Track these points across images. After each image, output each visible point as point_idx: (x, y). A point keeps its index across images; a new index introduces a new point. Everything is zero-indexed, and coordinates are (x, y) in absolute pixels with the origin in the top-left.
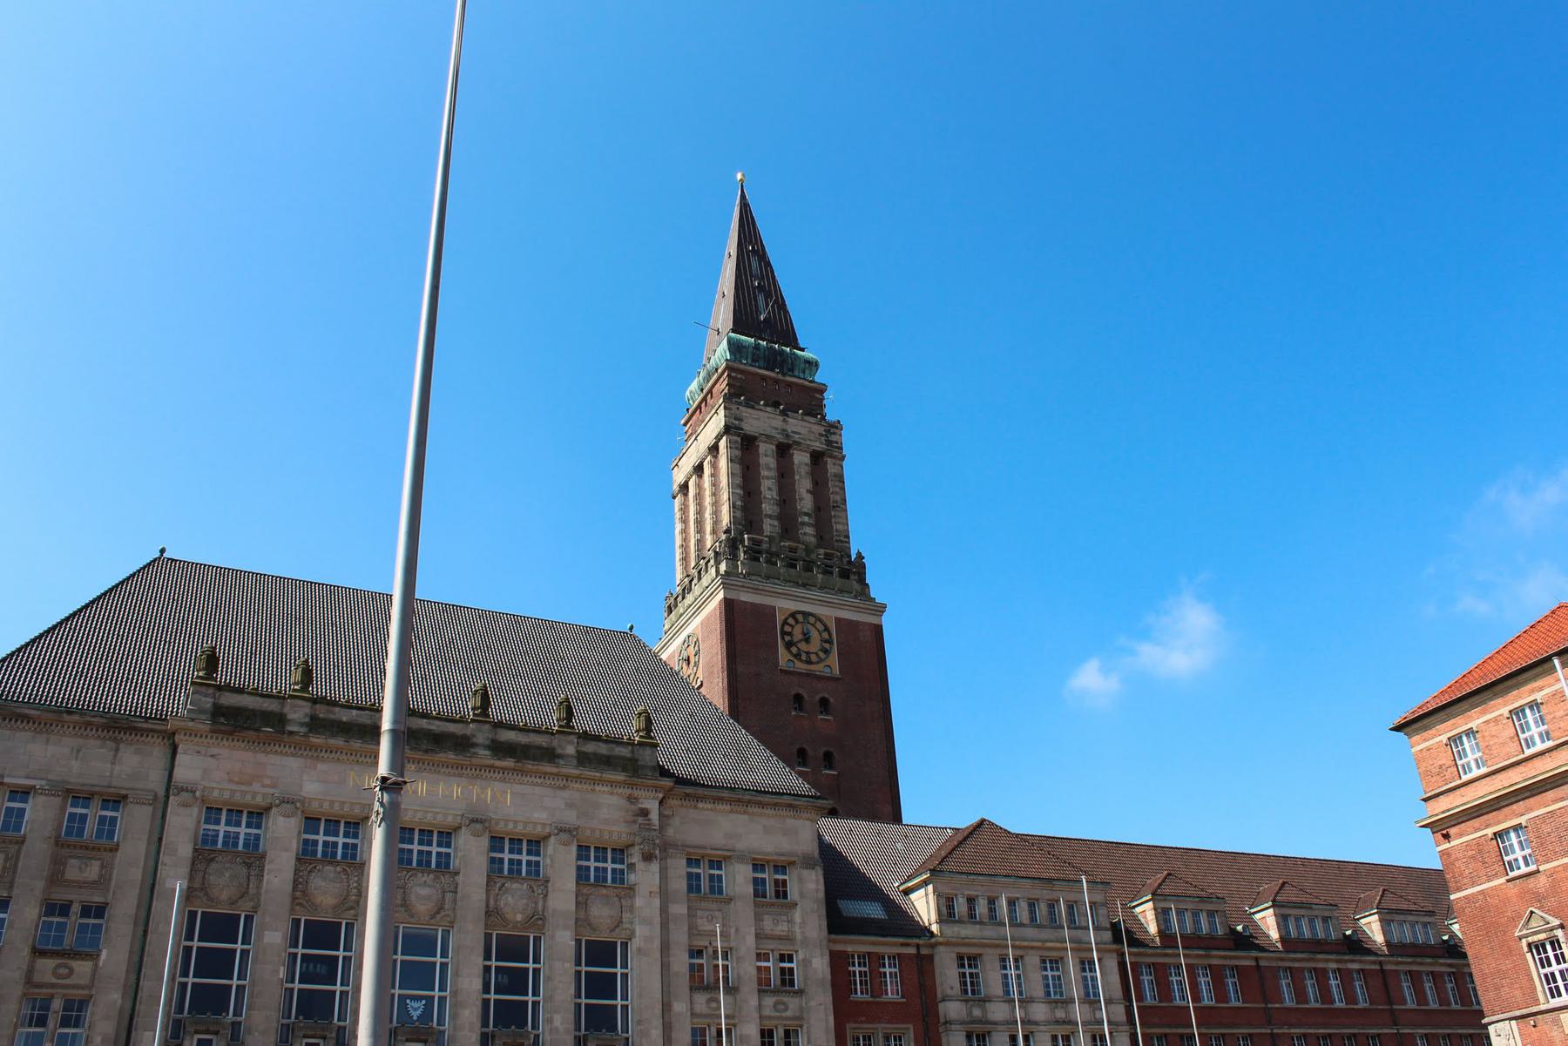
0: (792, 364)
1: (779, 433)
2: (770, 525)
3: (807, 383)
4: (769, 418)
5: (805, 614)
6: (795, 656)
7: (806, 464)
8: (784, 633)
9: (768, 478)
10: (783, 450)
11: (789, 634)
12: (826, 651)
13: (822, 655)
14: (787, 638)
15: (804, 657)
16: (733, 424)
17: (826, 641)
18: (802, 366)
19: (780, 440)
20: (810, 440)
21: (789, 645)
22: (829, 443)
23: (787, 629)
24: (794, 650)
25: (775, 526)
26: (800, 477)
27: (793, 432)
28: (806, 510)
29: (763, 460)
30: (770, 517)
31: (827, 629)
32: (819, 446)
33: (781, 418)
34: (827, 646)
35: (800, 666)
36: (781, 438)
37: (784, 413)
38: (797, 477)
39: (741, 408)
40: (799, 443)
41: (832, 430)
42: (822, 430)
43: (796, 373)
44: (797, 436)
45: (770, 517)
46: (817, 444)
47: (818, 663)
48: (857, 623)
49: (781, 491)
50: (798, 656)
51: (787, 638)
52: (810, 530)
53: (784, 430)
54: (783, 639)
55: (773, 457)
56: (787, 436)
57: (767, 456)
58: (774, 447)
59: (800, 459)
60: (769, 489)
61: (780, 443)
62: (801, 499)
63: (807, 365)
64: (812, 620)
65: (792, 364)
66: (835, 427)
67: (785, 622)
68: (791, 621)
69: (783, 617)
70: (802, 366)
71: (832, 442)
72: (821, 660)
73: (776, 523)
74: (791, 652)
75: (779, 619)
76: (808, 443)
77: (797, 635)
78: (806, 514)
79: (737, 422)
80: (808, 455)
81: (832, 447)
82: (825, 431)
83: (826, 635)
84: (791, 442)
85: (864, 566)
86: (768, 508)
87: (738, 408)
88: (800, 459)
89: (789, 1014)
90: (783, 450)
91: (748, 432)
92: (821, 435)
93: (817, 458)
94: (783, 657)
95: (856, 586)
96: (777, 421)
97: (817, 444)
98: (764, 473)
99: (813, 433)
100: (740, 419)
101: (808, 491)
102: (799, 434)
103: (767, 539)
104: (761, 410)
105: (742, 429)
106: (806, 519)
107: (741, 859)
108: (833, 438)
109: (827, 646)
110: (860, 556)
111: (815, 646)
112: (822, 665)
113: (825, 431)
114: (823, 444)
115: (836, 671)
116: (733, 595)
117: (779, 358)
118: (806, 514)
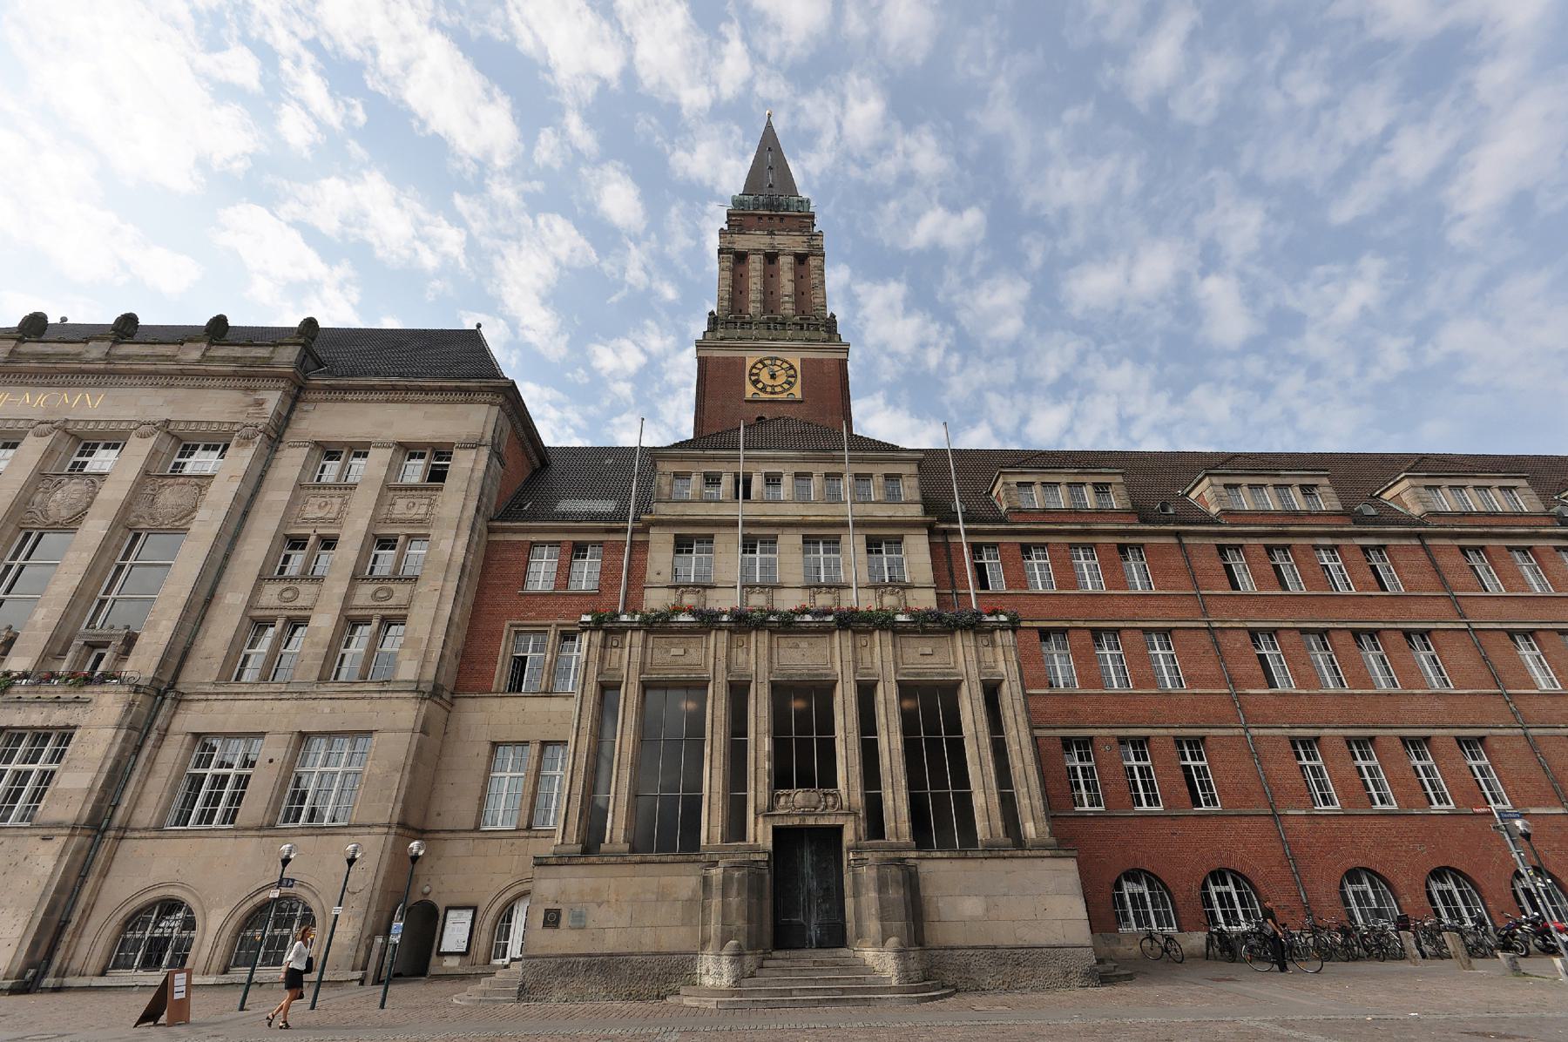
0: (788, 205)
5: (771, 359)
6: (760, 390)
8: (751, 374)
9: (754, 277)
10: (771, 258)
11: (757, 374)
12: (789, 383)
13: (786, 386)
14: (753, 378)
15: (769, 389)
17: (792, 376)
18: (796, 204)
21: (755, 383)
23: (754, 371)
24: (760, 385)
30: (754, 302)
31: (791, 367)
32: (801, 249)
34: (792, 380)
35: (763, 396)
37: (771, 233)
41: (814, 238)
45: (754, 302)
47: (781, 392)
48: (821, 361)
49: (766, 284)
50: (763, 389)
51: (753, 378)
52: (788, 306)
54: (750, 379)
57: (755, 264)
59: (785, 262)
60: (755, 284)
64: (779, 363)
65: (788, 205)
66: (820, 234)
67: (754, 367)
68: (760, 366)
69: (752, 364)
71: (814, 245)
72: (785, 390)
73: (758, 305)
75: (749, 364)
77: (764, 376)
80: (792, 257)
83: (792, 372)
85: (835, 322)
88: (785, 262)
89: (391, 602)
90: (771, 258)
93: (801, 259)
94: (750, 390)
95: (825, 335)
96: (767, 239)
107: (383, 446)
108: (815, 243)
109: (792, 380)
110: (833, 316)
111: (781, 379)
112: (786, 394)
115: (798, 396)
116: (704, 354)
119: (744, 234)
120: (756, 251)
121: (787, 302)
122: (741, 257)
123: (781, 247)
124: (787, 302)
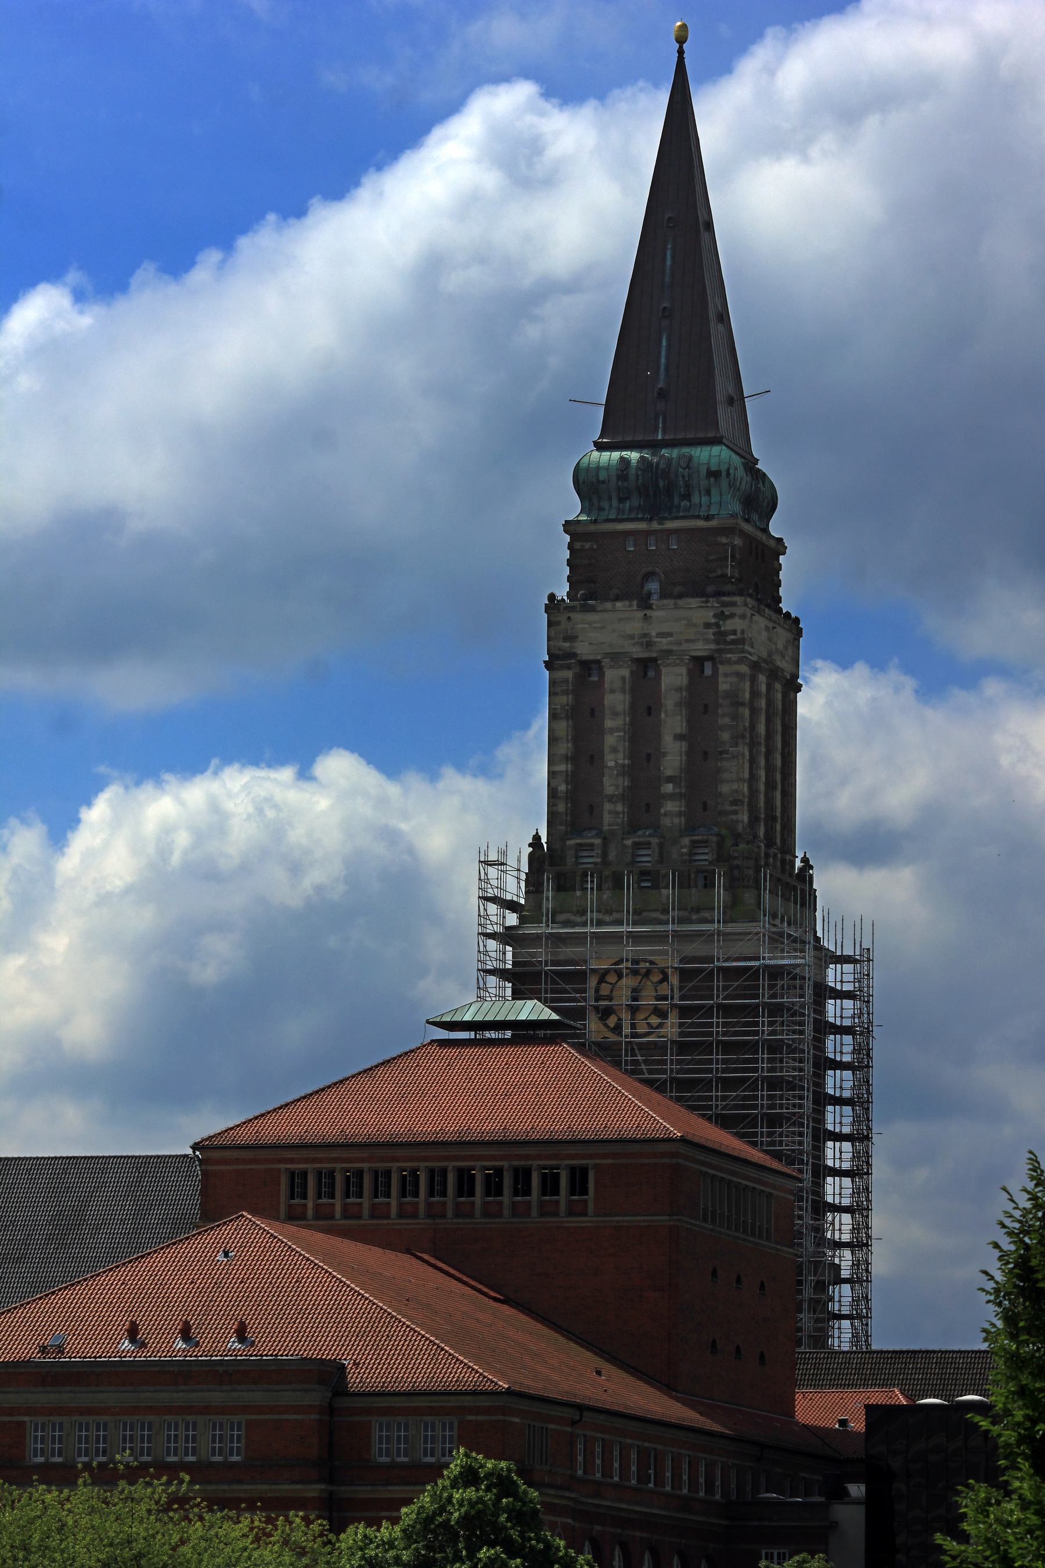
1: (634, 644)
2: (610, 812)
3: (701, 523)
4: (620, 620)
7: (679, 689)
16: (560, 649)
18: (704, 483)
19: (641, 656)
20: (687, 641)
22: (720, 636)
25: (617, 813)
26: (666, 715)
27: (660, 635)
28: (669, 772)
29: (609, 699)
30: (611, 799)
32: (701, 648)
33: (640, 614)
36: (638, 652)
37: (645, 603)
38: (663, 715)
39: (573, 615)
40: (670, 652)
42: (709, 616)
43: (696, 499)
44: (664, 640)
45: (611, 799)
46: (700, 645)
53: (645, 635)
55: (624, 691)
56: (649, 645)
58: (626, 672)
60: (614, 750)
61: (638, 661)
62: (665, 754)
63: (712, 480)
65: (688, 486)
70: (704, 483)
71: (724, 634)
73: (619, 808)
74: (606, 1026)
76: (685, 647)
78: (670, 779)
79: (567, 644)
80: (683, 670)
81: (726, 642)
82: (715, 616)
84: (654, 655)
86: (612, 784)
87: (569, 618)
91: (584, 658)
92: (707, 625)
97: (700, 645)
98: (609, 723)
99: (695, 625)
100: (571, 638)
101: (679, 737)
102: (670, 634)
103: (598, 841)
104: (605, 611)
105: (574, 655)
106: (669, 788)
113: (715, 616)
114: (707, 641)
117: (661, 484)
118: (670, 779)
119: (593, 609)
120: (616, 657)
121: (671, 797)
122: (588, 668)
123: (664, 643)
124: (671, 797)
